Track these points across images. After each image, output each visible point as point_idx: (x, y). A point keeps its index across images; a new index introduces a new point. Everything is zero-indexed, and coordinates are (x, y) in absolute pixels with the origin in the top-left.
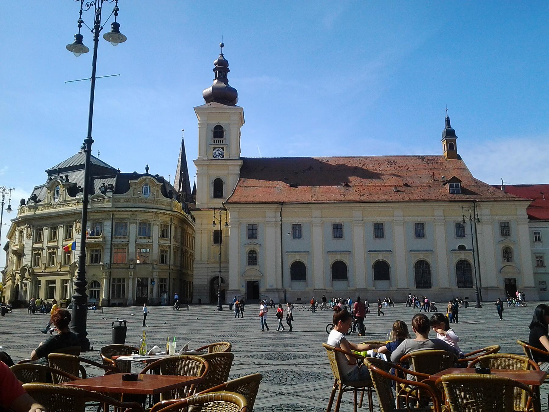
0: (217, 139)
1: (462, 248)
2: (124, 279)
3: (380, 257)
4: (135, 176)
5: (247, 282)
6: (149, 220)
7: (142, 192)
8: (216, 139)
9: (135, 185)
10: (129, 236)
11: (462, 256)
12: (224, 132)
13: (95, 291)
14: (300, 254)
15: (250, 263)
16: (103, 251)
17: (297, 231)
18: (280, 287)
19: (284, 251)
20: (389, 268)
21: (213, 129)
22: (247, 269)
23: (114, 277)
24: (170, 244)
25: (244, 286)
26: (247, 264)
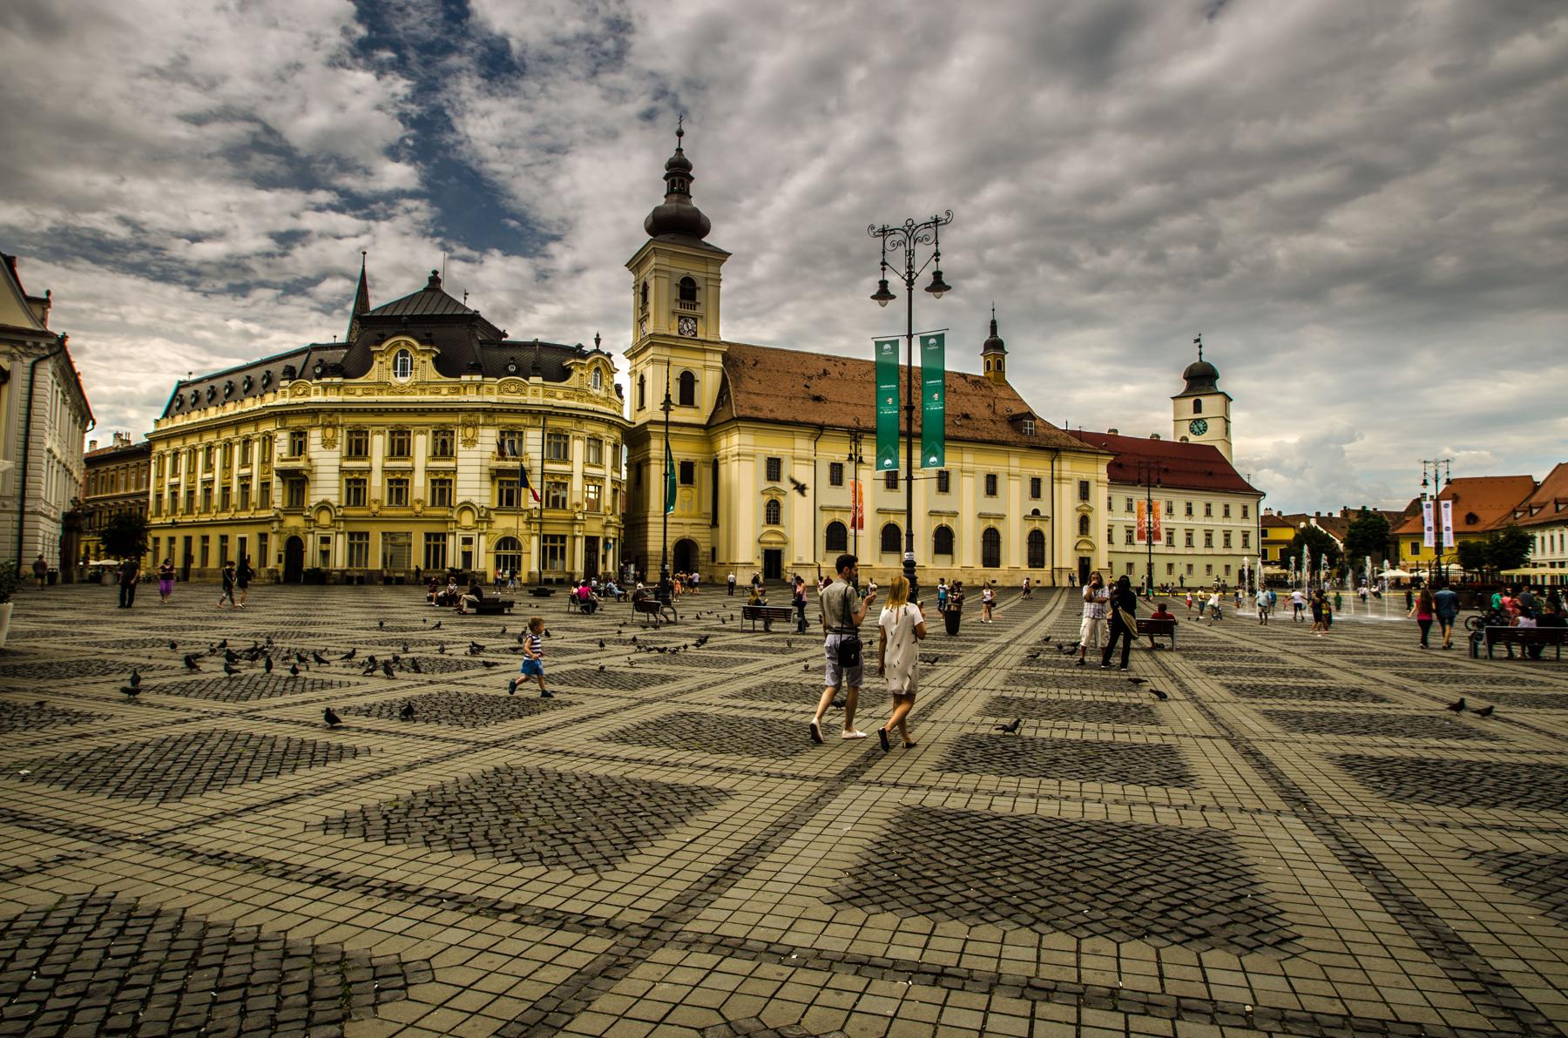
0: (686, 302)
1: (1036, 512)
2: (563, 538)
3: (944, 521)
4: (578, 352)
11: (1037, 525)
13: (506, 557)
15: (769, 522)
19: (818, 506)
22: (766, 529)
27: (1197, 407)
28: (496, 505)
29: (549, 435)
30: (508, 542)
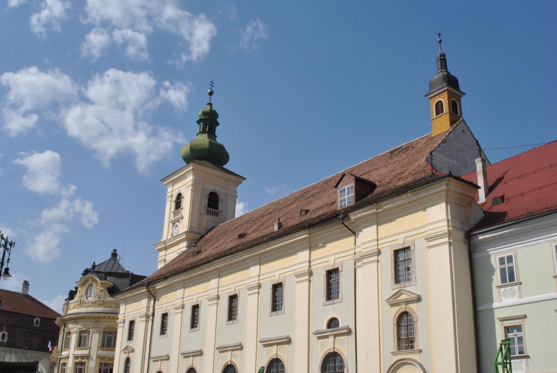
1: (333, 323)
10: (70, 348)
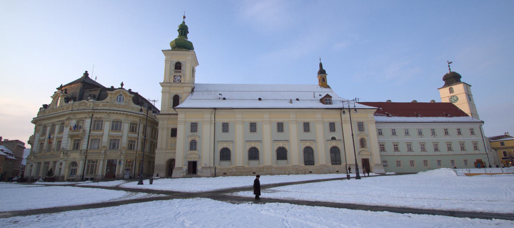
0: (177, 70)
3: (281, 145)
4: (112, 89)
5: (189, 162)
6: (121, 119)
7: (116, 100)
8: (176, 70)
9: (111, 95)
10: (103, 130)
11: (334, 144)
12: (182, 66)
14: (226, 143)
15: (191, 150)
16: (82, 140)
17: (225, 127)
18: (212, 165)
19: (216, 140)
20: (286, 152)
21: (175, 64)
22: (189, 153)
23: (89, 159)
24: (138, 136)
25: (186, 165)
26: (189, 149)
27: (451, 91)
28: (71, 149)
29: (95, 121)
30: (74, 164)
